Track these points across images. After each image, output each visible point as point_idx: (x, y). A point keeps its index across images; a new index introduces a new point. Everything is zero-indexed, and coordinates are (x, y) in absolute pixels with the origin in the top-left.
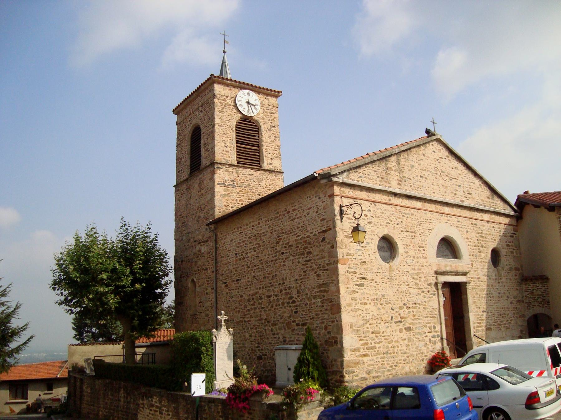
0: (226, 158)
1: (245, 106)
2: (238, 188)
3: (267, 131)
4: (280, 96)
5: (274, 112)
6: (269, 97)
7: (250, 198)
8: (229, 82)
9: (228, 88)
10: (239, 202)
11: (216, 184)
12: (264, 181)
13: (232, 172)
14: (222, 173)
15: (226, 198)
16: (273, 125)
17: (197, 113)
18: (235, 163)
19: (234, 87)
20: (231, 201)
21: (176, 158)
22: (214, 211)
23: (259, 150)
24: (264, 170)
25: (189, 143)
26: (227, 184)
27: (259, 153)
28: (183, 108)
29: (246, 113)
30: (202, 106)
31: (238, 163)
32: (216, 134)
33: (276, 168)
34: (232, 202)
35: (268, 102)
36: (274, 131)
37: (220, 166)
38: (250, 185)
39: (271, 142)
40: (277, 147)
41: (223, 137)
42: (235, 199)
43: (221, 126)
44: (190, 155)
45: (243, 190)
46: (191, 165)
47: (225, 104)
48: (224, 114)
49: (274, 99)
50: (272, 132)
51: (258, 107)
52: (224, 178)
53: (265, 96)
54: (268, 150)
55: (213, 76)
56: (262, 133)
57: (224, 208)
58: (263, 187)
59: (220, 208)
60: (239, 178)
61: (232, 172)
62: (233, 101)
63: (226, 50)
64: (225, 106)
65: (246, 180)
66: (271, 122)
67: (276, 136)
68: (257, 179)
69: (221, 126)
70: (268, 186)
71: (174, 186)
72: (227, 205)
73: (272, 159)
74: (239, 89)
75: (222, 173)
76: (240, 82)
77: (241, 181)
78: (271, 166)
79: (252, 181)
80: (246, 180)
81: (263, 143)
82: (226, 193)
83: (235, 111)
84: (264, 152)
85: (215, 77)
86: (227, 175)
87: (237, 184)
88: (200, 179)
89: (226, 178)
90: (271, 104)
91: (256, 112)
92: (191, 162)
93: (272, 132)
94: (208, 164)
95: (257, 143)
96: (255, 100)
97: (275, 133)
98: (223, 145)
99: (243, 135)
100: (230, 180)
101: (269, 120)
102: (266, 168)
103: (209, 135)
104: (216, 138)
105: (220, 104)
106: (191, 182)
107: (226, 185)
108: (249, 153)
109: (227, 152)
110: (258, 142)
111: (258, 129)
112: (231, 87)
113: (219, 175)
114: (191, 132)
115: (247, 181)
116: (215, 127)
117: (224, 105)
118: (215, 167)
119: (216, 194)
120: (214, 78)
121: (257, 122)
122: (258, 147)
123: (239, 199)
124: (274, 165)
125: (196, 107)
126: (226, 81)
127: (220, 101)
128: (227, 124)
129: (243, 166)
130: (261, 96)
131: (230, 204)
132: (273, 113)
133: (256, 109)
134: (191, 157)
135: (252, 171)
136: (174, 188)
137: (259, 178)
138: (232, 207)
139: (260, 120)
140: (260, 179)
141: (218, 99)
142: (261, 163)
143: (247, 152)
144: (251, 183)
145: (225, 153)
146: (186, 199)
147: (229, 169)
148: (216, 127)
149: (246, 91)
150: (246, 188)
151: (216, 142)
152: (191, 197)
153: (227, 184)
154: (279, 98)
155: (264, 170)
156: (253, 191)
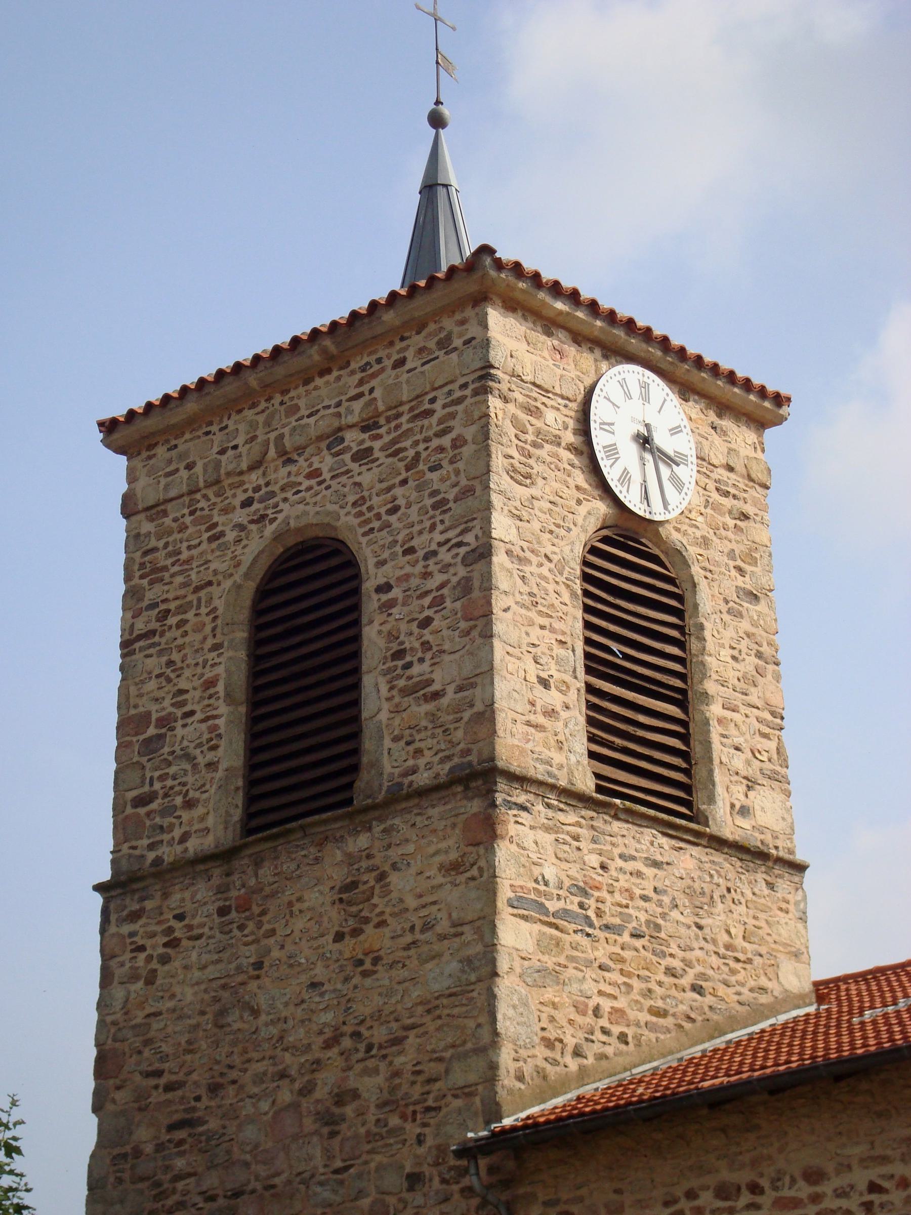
0: (546, 754)
1: (630, 452)
2: (601, 935)
3: (726, 617)
4: (780, 420)
5: (749, 509)
6: (726, 423)
7: (660, 1003)
8: (559, 305)
9: (549, 342)
10: (607, 1025)
11: (501, 903)
12: (720, 907)
13: (576, 838)
14: (528, 836)
15: (549, 994)
16: (746, 583)
17: (326, 463)
18: (587, 784)
19: (579, 338)
20: (573, 1016)
21: (113, 718)
22: (494, 1067)
23: (684, 724)
24: (718, 843)
25: (241, 635)
26: (553, 906)
27: (685, 738)
28: (191, 423)
29: (632, 500)
30: (368, 426)
31: (599, 789)
32: (499, 602)
33: (768, 838)
34: (579, 1019)
35: (724, 448)
36: (754, 624)
37: (522, 798)
38: (658, 927)
39: (740, 686)
40: (769, 717)
41: (531, 624)
42: (592, 1004)
43: (520, 559)
44: (243, 709)
45: (627, 954)
46: (252, 766)
47: (538, 433)
48: (534, 491)
49: (751, 436)
50: (745, 625)
51: (687, 473)
52: (536, 871)
53: (712, 416)
54: (733, 731)
55: (488, 261)
56: (701, 627)
57: (541, 1052)
58: (714, 941)
59: (523, 1053)
60: (603, 879)
61: (576, 838)
62: (571, 423)
63: (445, 110)
64: (535, 445)
65: (638, 892)
66: (739, 569)
67: (765, 649)
68: (689, 892)
69: (520, 559)
70: (739, 942)
71: (98, 888)
72: (552, 1034)
73: (751, 784)
74: (598, 352)
75: (528, 836)
76: (611, 316)
77: (618, 897)
78: (745, 823)
79: (666, 900)
80: (638, 892)
81: (710, 686)
82: (549, 961)
83: (580, 478)
84: (715, 738)
85: (499, 264)
86: (550, 850)
87: (599, 913)
88: (351, 859)
89: (550, 872)
90: (740, 468)
91: (678, 501)
92: (252, 751)
93: (745, 625)
94: (423, 778)
95: (678, 683)
96: (675, 431)
97: (759, 632)
98: (533, 671)
99: (613, 628)
100: (567, 883)
101: (731, 555)
102: (728, 833)
103: (438, 602)
104: (499, 627)
105: (512, 432)
106: (266, 872)
107: (546, 912)
108: (641, 733)
109: (551, 713)
110: (682, 677)
111: (680, 598)
112: (562, 334)
113: (514, 848)
114: (260, 572)
115: (645, 898)
116: (495, 559)
117: (530, 437)
118: (499, 798)
119: (503, 965)
120: (493, 273)
121: (678, 554)
122: (682, 704)
123: (606, 1005)
124: (762, 819)
125: (317, 425)
126: (549, 299)
127: (511, 408)
128: (549, 549)
129: (628, 811)
130: (694, 408)
131: (569, 1030)
132: (745, 517)
133: (678, 484)
134: (253, 720)
135: (664, 841)
136: (98, 900)
137: (697, 886)
138: (577, 1053)
139: (692, 551)
140: (703, 893)
141: (506, 400)
142: (699, 799)
143: (630, 729)
144: (664, 916)
145: (541, 719)
146: (212, 972)
147: (561, 817)
148: (499, 559)
149: (633, 373)
150: (638, 943)
151: (499, 647)
152: (259, 965)
153: (553, 906)
154: (770, 433)
155: (718, 843)
156: (669, 961)
